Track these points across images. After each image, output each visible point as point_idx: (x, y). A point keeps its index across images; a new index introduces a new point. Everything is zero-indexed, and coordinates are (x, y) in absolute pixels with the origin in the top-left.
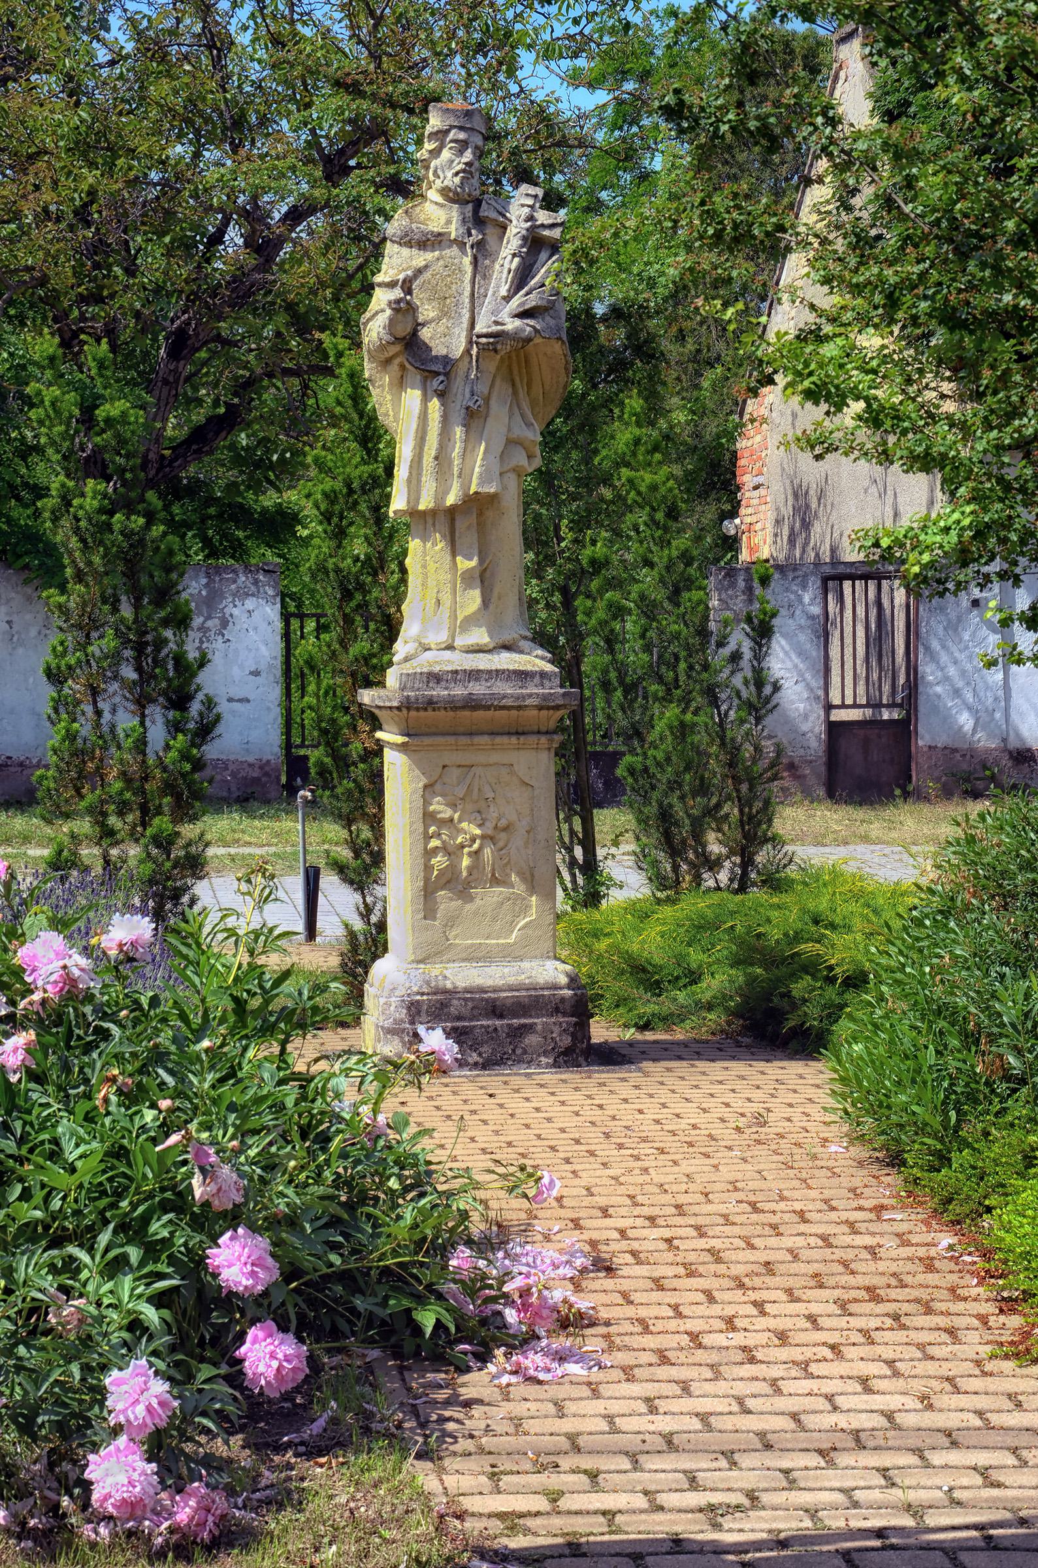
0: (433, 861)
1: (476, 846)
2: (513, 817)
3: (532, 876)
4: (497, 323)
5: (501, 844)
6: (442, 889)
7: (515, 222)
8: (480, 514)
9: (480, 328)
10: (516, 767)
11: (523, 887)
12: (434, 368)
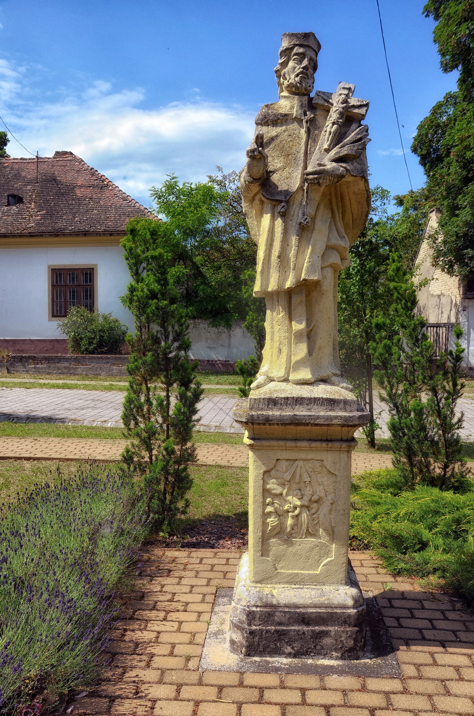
0: (269, 520)
1: (297, 512)
2: (322, 494)
3: (333, 532)
4: (320, 165)
5: (313, 511)
6: (274, 537)
7: (335, 104)
8: (308, 294)
9: (310, 169)
10: (325, 462)
11: (327, 538)
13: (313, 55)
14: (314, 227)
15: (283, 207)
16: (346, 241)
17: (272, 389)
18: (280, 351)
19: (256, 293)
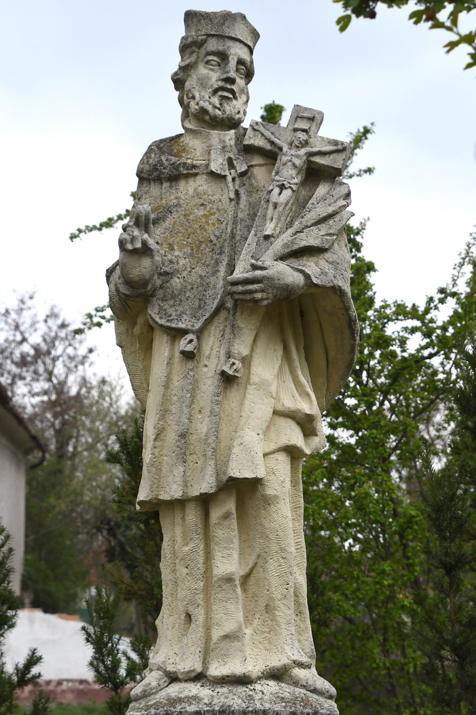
4: (255, 267)
7: (285, 149)
9: (238, 274)
12: (181, 325)
13: (244, 54)
14: (248, 379)
15: (191, 341)
16: (311, 401)
17: (173, 695)
18: (189, 617)
19: (141, 503)
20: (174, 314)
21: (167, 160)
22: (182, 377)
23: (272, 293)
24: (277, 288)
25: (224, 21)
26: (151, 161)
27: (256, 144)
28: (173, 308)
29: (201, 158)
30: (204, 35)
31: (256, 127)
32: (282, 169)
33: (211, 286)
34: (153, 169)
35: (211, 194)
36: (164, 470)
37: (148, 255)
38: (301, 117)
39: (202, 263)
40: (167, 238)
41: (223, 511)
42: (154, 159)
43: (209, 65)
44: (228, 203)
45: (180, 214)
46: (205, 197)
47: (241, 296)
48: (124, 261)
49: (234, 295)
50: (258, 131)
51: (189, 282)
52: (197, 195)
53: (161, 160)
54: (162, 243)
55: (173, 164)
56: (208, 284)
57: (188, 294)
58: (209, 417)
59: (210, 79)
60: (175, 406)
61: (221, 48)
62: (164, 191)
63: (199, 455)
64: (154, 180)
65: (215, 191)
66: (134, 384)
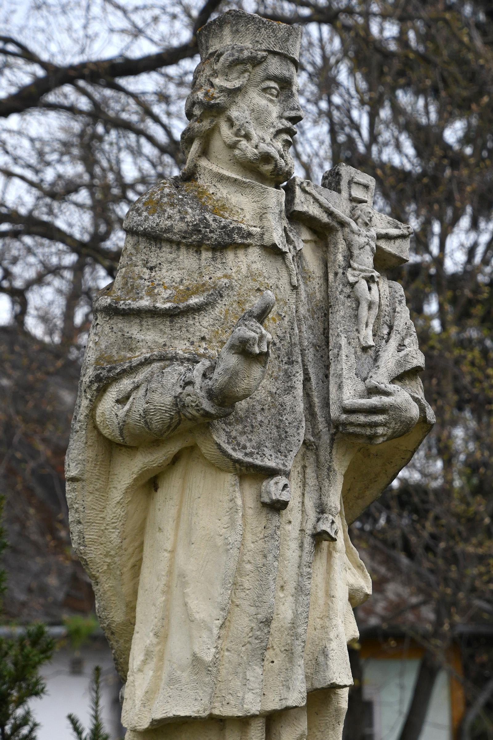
20: (248, 444)
21: (215, 220)
22: (262, 536)
23: (394, 428)
24: (401, 422)
25: (288, 36)
26: (188, 218)
27: (311, 212)
28: (245, 437)
29: (252, 224)
30: (265, 51)
31: (307, 189)
32: (360, 254)
33: (288, 408)
34: (193, 230)
35: (267, 276)
36: (223, 672)
37: (260, 362)
38: (356, 183)
39: (269, 374)
40: (217, 332)
41: (298, 733)
42: (194, 216)
43: (266, 93)
44: (289, 292)
45: (231, 300)
46: (260, 279)
47: (358, 430)
48: (237, 368)
49: (348, 427)
50: (310, 194)
51: (258, 401)
52: (252, 275)
53: (205, 218)
54: (211, 339)
55: (224, 227)
56: (282, 406)
57: (259, 418)
58: (293, 596)
59: (269, 113)
60: (248, 577)
61: (287, 74)
62: (203, 263)
63: (277, 650)
64: (188, 246)
65: (270, 272)
66: (87, 537)
